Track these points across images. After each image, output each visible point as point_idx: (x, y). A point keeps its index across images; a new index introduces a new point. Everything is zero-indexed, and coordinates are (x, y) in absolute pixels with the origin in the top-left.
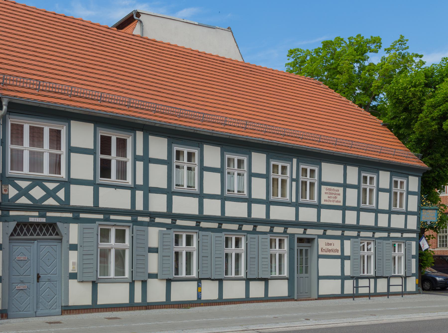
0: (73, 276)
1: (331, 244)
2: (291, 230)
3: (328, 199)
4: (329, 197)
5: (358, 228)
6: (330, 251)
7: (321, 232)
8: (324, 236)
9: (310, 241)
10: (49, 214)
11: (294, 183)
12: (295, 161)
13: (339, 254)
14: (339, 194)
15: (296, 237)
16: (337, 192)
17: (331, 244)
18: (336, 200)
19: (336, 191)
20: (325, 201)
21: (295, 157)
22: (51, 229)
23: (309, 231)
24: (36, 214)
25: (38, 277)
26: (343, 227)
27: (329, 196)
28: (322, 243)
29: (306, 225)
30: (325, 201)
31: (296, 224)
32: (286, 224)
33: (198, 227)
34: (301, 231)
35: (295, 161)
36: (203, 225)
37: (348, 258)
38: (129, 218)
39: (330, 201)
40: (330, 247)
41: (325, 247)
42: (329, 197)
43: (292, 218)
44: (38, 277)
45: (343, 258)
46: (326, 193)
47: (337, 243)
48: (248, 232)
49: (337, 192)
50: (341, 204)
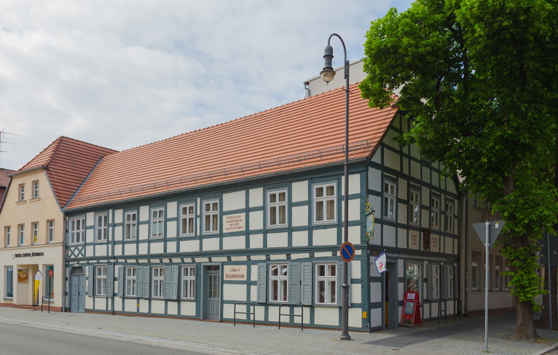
0: (87, 293)
1: (236, 270)
2: (198, 260)
3: (229, 227)
4: (230, 225)
5: (266, 251)
6: (235, 276)
7: (225, 259)
8: (230, 262)
9: (217, 268)
10: (80, 262)
11: (198, 219)
12: (199, 200)
13: (245, 279)
14: (241, 220)
15: (203, 264)
16: (238, 219)
17: (236, 270)
18: (238, 226)
19: (238, 217)
20: (226, 229)
21: (199, 196)
22: (80, 268)
23: (214, 259)
24: (76, 262)
25: (79, 294)
26: (248, 252)
27: (231, 223)
28: (227, 269)
29: (210, 254)
30: (226, 229)
31: (201, 254)
32: (192, 255)
33: (138, 263)
34: (206, 260)
35: (199, 200)
36: (141, 261)
37: (255, 283)
38: (106, 261)
39: (232, 228)
40: (235, 273)
41: (230, 273)
42: (230, 225)
43: (197, 249)
44: (79, 294)
45: (249, 283)
46: (227, 222)
47: (243, 269)
48: (166, 264)
49: (238, 219)
50: (244, 229)
